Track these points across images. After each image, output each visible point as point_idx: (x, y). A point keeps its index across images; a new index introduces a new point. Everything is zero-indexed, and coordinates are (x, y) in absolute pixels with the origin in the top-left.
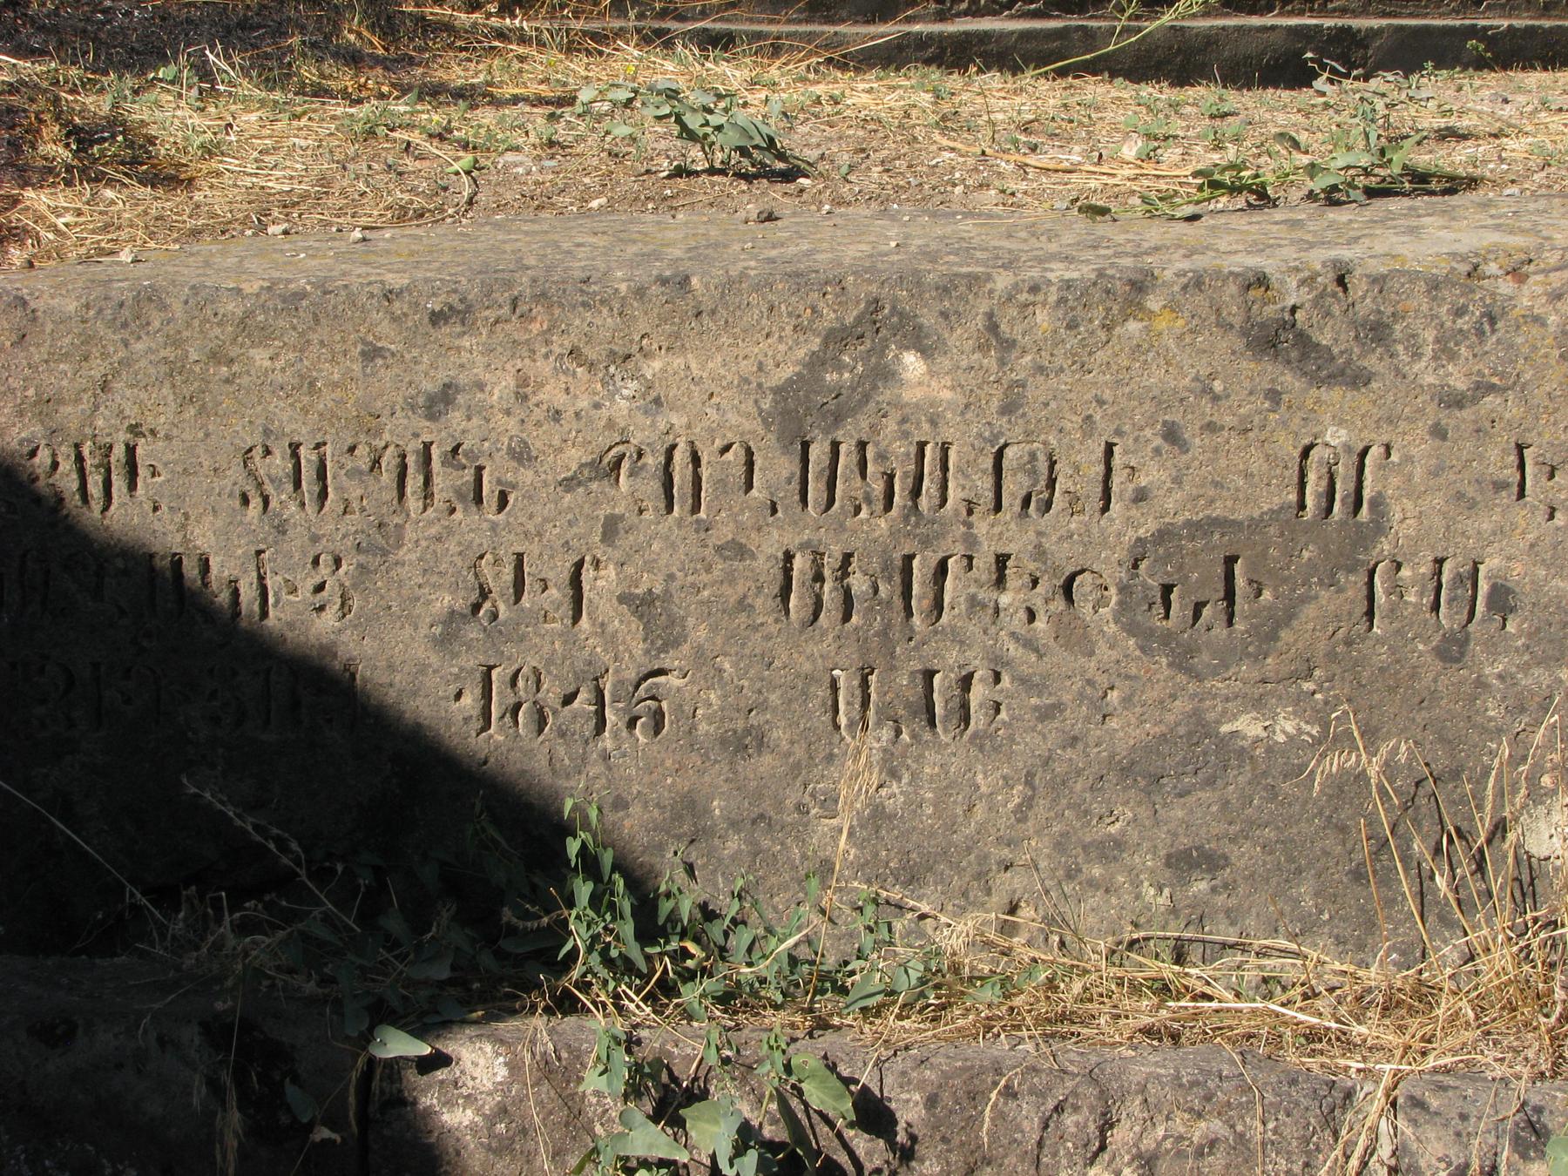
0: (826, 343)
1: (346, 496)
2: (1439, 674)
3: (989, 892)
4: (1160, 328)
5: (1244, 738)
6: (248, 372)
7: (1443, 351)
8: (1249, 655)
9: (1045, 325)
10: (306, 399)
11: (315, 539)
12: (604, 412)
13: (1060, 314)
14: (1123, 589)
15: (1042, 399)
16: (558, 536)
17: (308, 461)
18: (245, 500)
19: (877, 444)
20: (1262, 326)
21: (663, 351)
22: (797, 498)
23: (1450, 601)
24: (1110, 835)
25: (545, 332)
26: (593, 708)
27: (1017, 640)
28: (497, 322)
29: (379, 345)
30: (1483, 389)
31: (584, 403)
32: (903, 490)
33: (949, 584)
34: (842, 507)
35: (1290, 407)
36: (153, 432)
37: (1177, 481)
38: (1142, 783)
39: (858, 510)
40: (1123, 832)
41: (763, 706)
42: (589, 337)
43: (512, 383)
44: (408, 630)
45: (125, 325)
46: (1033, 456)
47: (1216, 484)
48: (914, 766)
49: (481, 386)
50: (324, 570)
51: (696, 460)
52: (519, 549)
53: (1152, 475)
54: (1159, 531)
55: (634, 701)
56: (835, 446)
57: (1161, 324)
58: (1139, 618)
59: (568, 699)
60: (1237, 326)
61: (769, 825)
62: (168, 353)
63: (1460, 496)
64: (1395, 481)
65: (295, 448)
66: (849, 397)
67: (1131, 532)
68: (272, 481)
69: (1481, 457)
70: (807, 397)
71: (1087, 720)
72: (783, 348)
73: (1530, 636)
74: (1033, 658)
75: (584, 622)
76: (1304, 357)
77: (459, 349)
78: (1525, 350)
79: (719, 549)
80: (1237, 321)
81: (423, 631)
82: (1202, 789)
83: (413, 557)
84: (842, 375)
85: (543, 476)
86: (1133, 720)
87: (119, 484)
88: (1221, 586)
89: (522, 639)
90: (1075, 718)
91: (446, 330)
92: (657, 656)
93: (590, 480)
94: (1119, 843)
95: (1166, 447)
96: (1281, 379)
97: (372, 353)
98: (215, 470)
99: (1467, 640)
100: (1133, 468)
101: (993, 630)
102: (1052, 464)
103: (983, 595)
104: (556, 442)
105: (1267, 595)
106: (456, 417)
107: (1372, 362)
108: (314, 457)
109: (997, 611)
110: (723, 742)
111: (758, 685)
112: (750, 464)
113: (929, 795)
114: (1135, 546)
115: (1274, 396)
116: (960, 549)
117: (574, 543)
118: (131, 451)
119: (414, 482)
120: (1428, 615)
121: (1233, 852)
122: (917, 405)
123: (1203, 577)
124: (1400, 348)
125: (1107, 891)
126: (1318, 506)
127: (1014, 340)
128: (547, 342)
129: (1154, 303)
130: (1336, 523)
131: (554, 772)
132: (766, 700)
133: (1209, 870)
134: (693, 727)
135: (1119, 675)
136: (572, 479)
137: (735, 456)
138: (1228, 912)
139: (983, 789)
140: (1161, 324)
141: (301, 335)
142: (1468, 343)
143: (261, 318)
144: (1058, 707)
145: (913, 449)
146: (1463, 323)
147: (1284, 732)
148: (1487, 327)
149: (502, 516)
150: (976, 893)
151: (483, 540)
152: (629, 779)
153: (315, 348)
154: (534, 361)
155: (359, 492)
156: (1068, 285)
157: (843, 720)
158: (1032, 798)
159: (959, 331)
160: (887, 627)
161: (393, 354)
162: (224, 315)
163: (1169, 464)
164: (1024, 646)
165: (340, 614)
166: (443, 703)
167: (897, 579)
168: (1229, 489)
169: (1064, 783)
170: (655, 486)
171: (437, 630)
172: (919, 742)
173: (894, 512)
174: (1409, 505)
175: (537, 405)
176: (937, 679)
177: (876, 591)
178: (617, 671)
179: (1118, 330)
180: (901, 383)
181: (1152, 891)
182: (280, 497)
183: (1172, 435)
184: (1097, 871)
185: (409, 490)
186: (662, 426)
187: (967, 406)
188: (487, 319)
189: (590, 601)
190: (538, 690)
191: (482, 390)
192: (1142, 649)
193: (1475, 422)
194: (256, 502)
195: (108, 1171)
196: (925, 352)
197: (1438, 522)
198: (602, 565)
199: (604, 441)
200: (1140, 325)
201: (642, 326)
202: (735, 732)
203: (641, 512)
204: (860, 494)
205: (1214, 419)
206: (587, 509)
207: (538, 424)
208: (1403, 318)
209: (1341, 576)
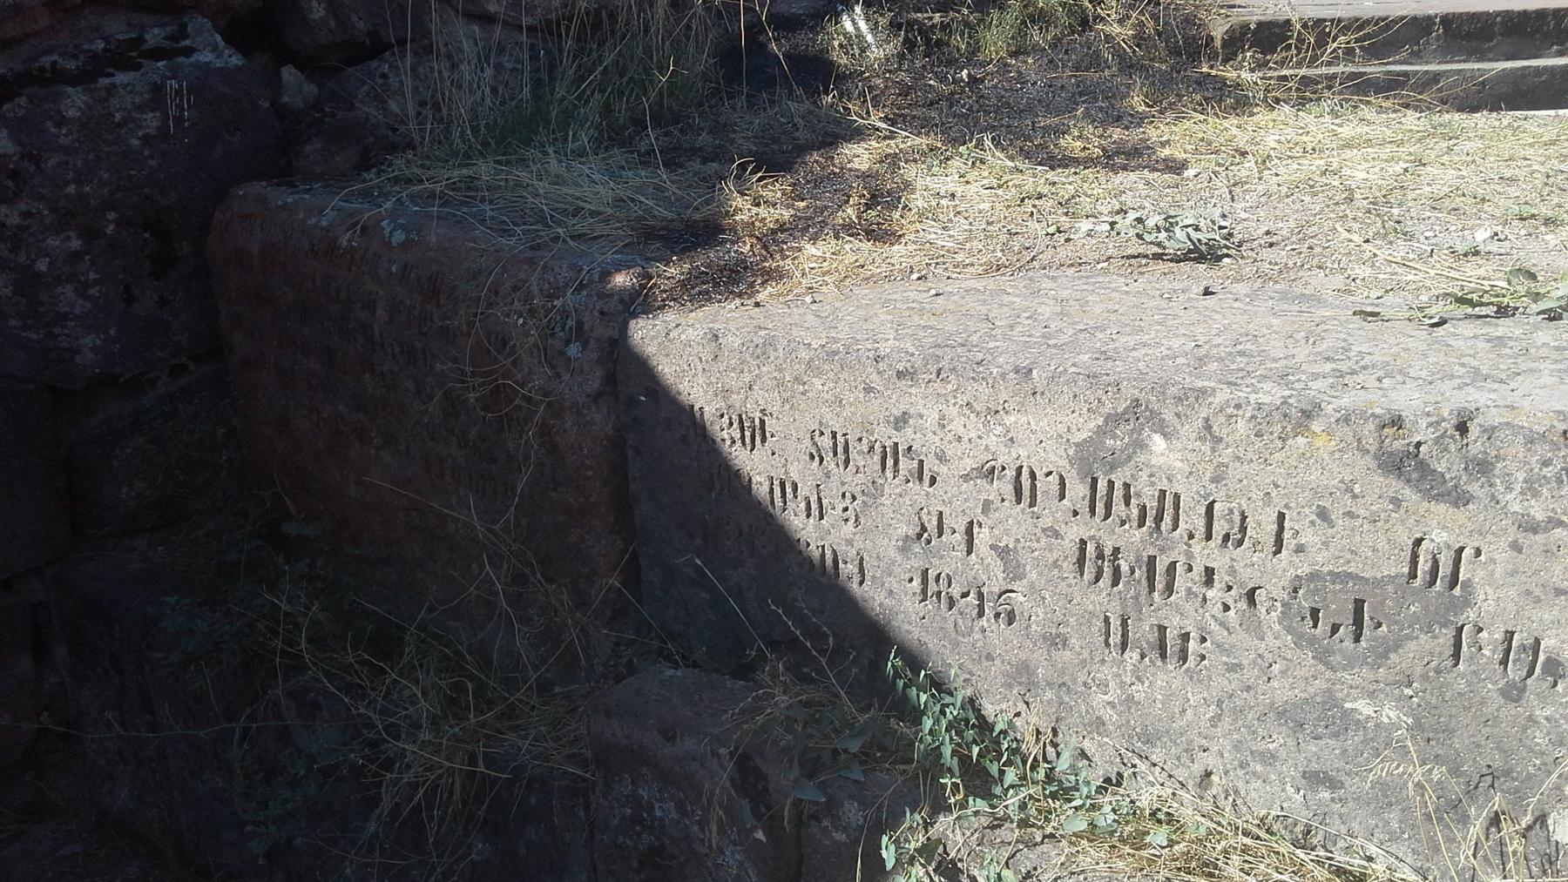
0: (1106, 421)
2: (1501, 707)
4: (1318, 445)
5: (1361, 714)
7: (1529, 489)
8: (1367, 663)
12: (984, 442)
15: (1238, 477)
22: (1088, 509)
26: (977, 602)
27: (1216, 620)
28: (929, 382)
31: (973, 435)
34: (1113, 520)
35: (1407, 511)
37: (1326, 544)
38: (1291, 725)
41: (1067, 624)
45: (758, 357)
46: (1231, 511)
49: (921, 416)
51: (1033, 475)
52: (941, 509)
53: (1307, 537)
56: (1111, 484)
58: (1294, 624)
59: (965, 595)
60: (1372, 453)
63: (1528, 593)
64: (1481, 573)
65: (834, 435)
66: (1120, 456)
70: (1094, 451)
71: (1258, 677)
72: (1081, 420)
74: (1226, 633)
76: (1422, 478)
79: (1044, 530)
80: (1373, 449)
81: (894, 543)
82: (1330, 738)
87: (758, 439)
90: (1250, 675)
91: (904, 382)
96: (1402, 491)
97: (868, 390)
102: (1244, 518)
105: (1384, 628)
106: (909, 431)
107: (1474, 488)
109: (1205, 599)
111: (1064, 611)
113: (1159, 697)
114: (1294, 580)
115: (1396, 502)
116: (1182, 559)
119: (890, 462)
120: (1497, 667)
121: (1348, 781)
122: (1160, 467)
123: (1338, 607)
125: (1264, 781)
126: (1424, 579)
128: (955, 397)
129: (1316, 426)
130: (1435, 592)
133: (1330, 788)
134: (1029, 626)
136: (967, 475)
137: (1054, 479)
138: (1341, 816)
139: (1192, 702)
140: (1319, 443)
141: (836, 374)
142: (1549, 486)
145: (1157, 494)
149: (931, 489)
151: (922, 501)
155: (863, 463)
156: (1259, 406)
163: (1320, 533)
164: (1220, 625)
168: (1361, 556)
171: (900, 543)
172: (1154, 665)
173: (1145, 529)
174: (1490, 591)
179: (1290, 442)
181: (1293, 790)
182: (828, 457)
183: (1323, 514)
184: (1259, 768)
186: (1014, 455)
187: (1191, 473)
190: (949, 586)
193: (1545, 545)
194: (817, 458)
197: (1511, 607)
203: (1003, 500)
205: (1353, 510)
207: (950, 442)
208: (1504, 460)
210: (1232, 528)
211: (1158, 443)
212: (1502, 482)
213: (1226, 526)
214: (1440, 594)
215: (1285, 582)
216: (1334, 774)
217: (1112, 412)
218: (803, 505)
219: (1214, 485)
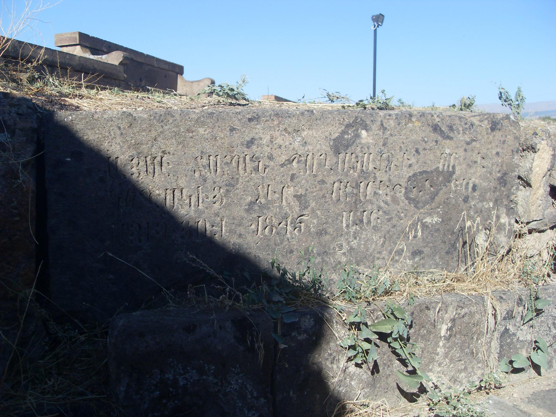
1: (223, 170)
11: (215, 183)
12: (292, 146)
13: (396, 121)
19: (356, 154)
21: (307, 129)
24: (400, 249)
25: (278, 124)
28: (266, 121)
29: (234, 127)
31: (287, 143)
36: (169, 153)
43: (269, 138)
45: (162, 121)
47: (425, 163)
48: (360, 235)
49: (261, 139)
53: (413, 160)
54: (414, 174)
59: (280, 224)
64: (457, 161)
67: (408, 175)
69: (472, 155)
72: (336, 129)
74: (387, 206)
78: (479, 132)
83: (241, 187)
86: (406, 220)
87: (157, 168)
92: (302, 211)
95: (416, 154)
96: (438, 138)
98: (187, 163)
104: (280, 153)
106: (254, 147)
107: (451, 135)
110: (317, 233)
111: (326, 217)
113: (363, 243)
114: (409, 178)
115: (436, 142)
116: (373, 180)
129: (414, 119)
134: (310, 230)
136: (283, 164)
139: (375, 240)
141: (213, 124)
143: (202, 119)
144: (392, 218)
148: (471, 127)
152: (294, 245)
153: (217, 128)
154: (275, 132)
155: (227, 169)
158: (385, 241)
159: (375, 125)
161: (238, 130)
162: (192, 119)
166: (247, 228)
170: (304, 165)
171: (247, 207)
172: (362, 230)
175: (275, 144)
178: (292, 216)
180: (361, 138)
183: (417, 151)
185: (240, 168)
186: (306, 149)
187: (376, 144)
188: (264, 120)
191: (261, 140)
193: (472, 148)
195: (206, 368)
196: (367, 130)
197: (464, 171)
201: (303, 123)
205: (425, 147)
207: (276, 149)
211: (364, 133)
215: (406, 180)
216: (421, 249)
217: (348, 123)
218: (187, 201)
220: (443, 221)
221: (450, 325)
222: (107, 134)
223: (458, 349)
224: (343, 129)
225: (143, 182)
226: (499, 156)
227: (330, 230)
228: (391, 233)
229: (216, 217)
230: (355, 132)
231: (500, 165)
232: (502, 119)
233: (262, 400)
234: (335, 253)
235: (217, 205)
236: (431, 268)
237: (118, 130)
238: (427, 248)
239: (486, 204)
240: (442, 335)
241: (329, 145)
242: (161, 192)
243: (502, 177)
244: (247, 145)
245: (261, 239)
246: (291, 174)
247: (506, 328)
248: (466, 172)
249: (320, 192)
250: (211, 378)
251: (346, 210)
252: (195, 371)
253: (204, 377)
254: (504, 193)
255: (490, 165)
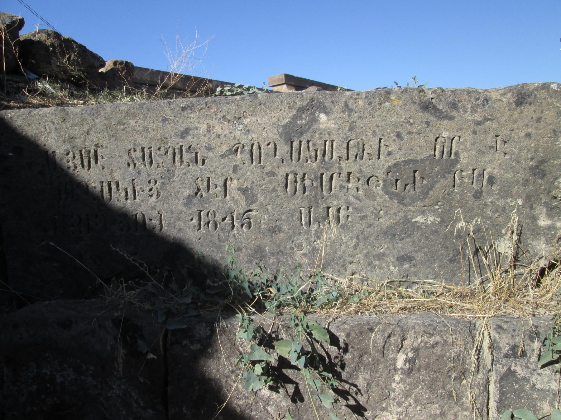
0: (297, 112)
2: (474, 202)
3: (346, 270)
4: (395, 104)
5: (419, 223)
6: (129, 127)
7: (473, 110)
8: (420, 199)
9: (362, 104)
10: (146, 134)
11: (149, 175)
12: (233, 135)
13: (366, 101)
14: (385, 181)
15: (361, 126)
16: (220, 172)
17: (147, 152)
18: (129, 165)
19: (313, 141)
20: (424, 102)
22: (290, 158)
23: (477, 181)
24: (381, 252)
25: (215, 112)
26: (231, 222)
28: (201, 109)
29: (167, 117)
30: (486, 120)
31: (227, 132)
32: (320, 154)
33: (334, 181)
34: (303, 160)
36: (102, 146)
37: (400, 149)
39: (307, 161)
40: (384, 251)
42: (228, 113)
44: (177, 201)
45: (93, 115)
46: (358, 143)
47: (411, 150)
49: (197, 128)
50: (152, 184)
51: (260, 148)
52: (209, 176)
53: (393, 147)
54: (395, 164)
55: (243, 219)
56: (301, 142)
57: (396, 103)
59: (224, 220)
61: (283, 254)
62: (106, 122)
63: (480, 150)
64: (462, 147)
65: (143, 149)
67: (386, 164)
68: (136, 159)
69: (486, 139)
70: (292, 128)
71: (374, 219)
72: (285, 114)
73: (499, 190)
74: (359, 202)
75: (228, 197)
77: (190, 117)
79: (267, 174)
80: (417, 101)
81: (181, 201)
82: (407, 238)
84: (302, 121)
85: (215, 154)
86: (387, 219)
87: (93, 161)
88: (412, 179)
89: (210, 202)
90: (371, 219)
91: (186, 112)
92: (249, 206)
93: (229, 155)
94: (383, 255)
95: (397, 139)
97: (165, 120)
98: (120, 156)
99: (482, 192)
100: (387, 146)
101: (347, 194)
103: (345, 184)
104: (219, 144)
105: (425, 182)
106: (189, 138)
107: (454, 114)
108: (148, 151)
109: (348, 189)
110: (269, 230)
111: (279, 213)
112: (276, 149)
113: (329, 243)
115: (428, 123)
116: (337, 171)
117: (225, 173)
118: (96, 152)
119: (178, 157)
121: (416, 255)
122: (324, 129)
123: (407, 175)
124: (461, 110)
126: (440, 155)
127: (353, 109)
128: (216, 115)
129: (393, 97)
131: (220, 241)
132: (281, 217)
133: (409, 261)
134: (260, 226)
135: (383, 206)
136: (224, 155)
137: (271, 146)
139: (344, 241)
140: (396, 103)
141: (144, 115)
143: (132, 111)
144: (366, 216)
145: (323, 142)
146: (479, 102)
147: (430, 221)
148: (485, 103)
149: (203, 166)
150: (342, 271)
152: (242, 242)
153: (148, 119)
155: (162, 161)
157: (303, 222)
158: (358, 243)
160: (316, 195)
161: (171, 120)
163: (397, 144)
165: (157, 197)
166: (187, 222)
167: (319, 180)
169: (367, 238)
170: (248, 156)
171: (185, 201)
173: (318, 161)
175: (213, 133)
176: (330, 210)
177: (313, 184)
178: (238, 211)
182: (139, 163)
183: (399, 135)
185: (176, 160)
186: (250, 138)
187: (339, 129)
189: (229, 190)
190: (215, 217)
191: (197, 130)
192: (390, 198)
193: (484, 129)
194: (132, 165)
195: (84, 368)
196: (327, 114)
197: (474, 159)
198: (233, 180)
199: (233, 143)
200: (389, 103)
202: (272, 227)
203: (244, 164)
204: (308, 156)
206: (228, 164)
207: (214, 139)
208: (461, 102)
209: (447, 175)
210: (359, 152)
211: (323, 117)
212: (463, 110)
213: (356, 150)
214: (447, 160)
218: (123, 194)
219: (350, 132)
220: (443, 221)
221: (410, 355)
222: (43, 130)
223: (425, 388)
224: (295, 113)
225: (79, 175)
226: (530, 138)
227: (285, 228)
228: (366, 234)
229: (154, 211)
230: (311, 116)
231: (533, 150)
232: (537, 89)
233: (150, 412)
234: (293, 253)
235: (154, 199)
236: (427, 278)
237: (52, 126)
238: (420, 253)
239: (511, 201)
240: (399, 367)
241: (277, 132)
242: (96, 185)
243: (537, 167)
244: (182, 135)
245: (203, 235)
246: (234, 166)
247: (509, 369)
248: (477, 160)
249: (269, 185)
250: (90, 379)
251: (303, 205)
252: (71, 369)
253: (83, 377)
254: (543, 187)
255: (516, 151)
